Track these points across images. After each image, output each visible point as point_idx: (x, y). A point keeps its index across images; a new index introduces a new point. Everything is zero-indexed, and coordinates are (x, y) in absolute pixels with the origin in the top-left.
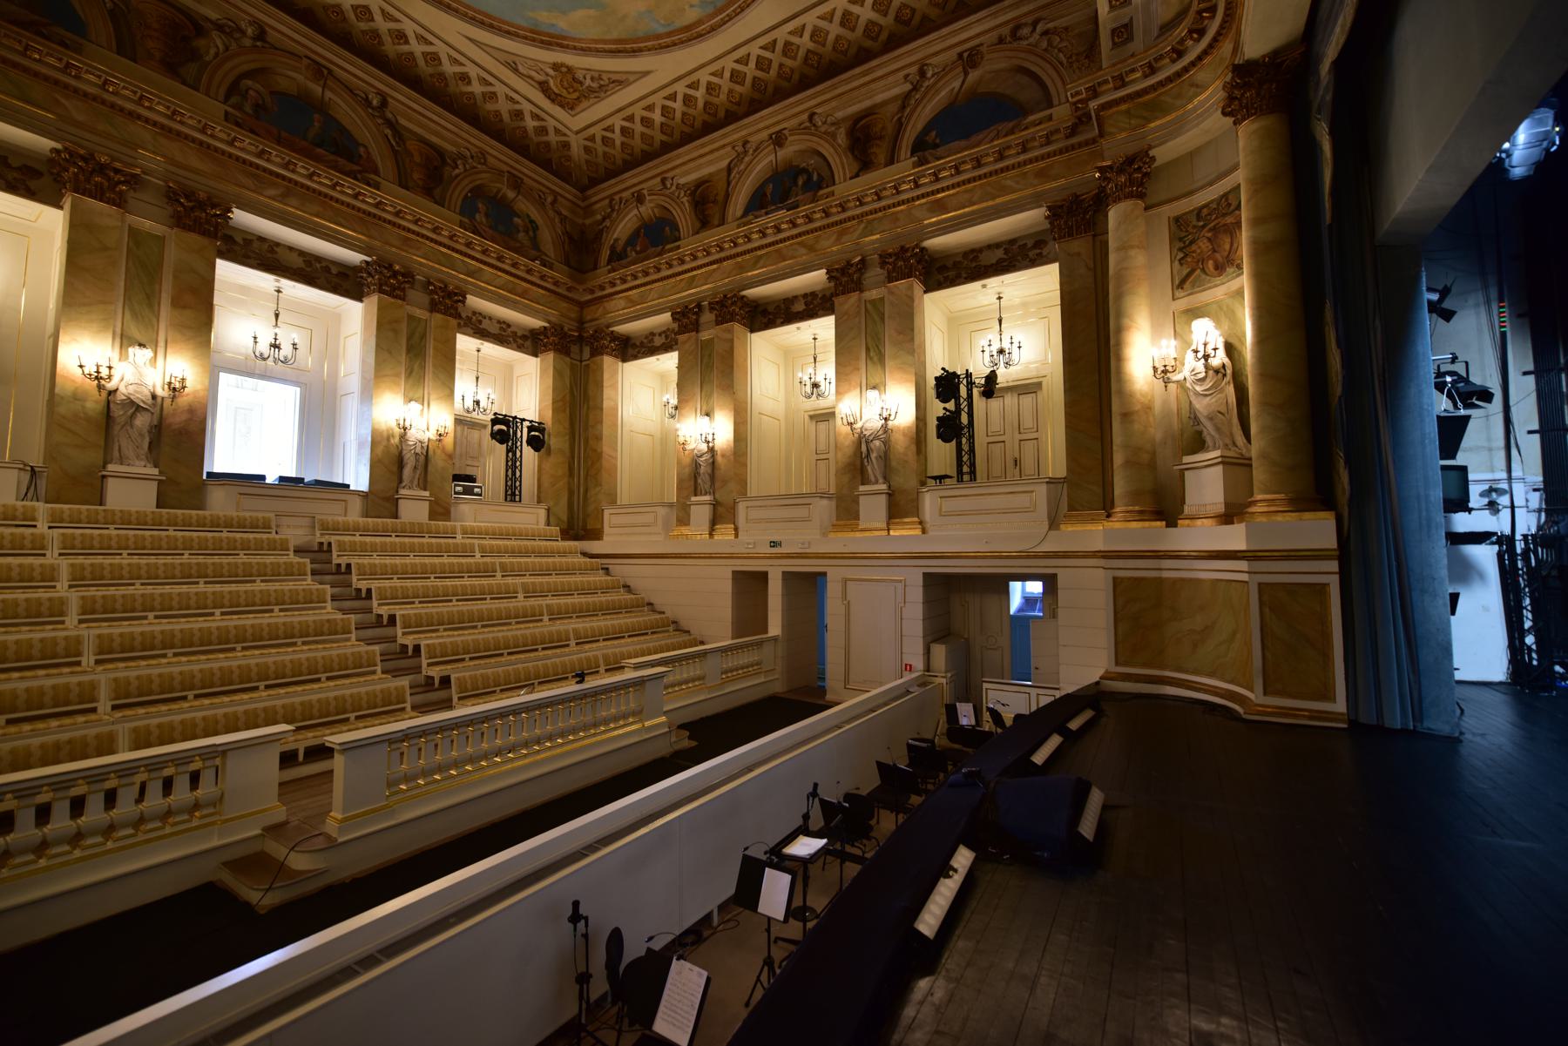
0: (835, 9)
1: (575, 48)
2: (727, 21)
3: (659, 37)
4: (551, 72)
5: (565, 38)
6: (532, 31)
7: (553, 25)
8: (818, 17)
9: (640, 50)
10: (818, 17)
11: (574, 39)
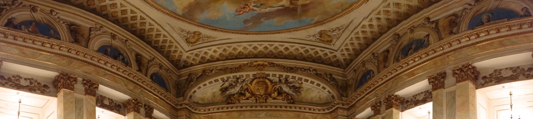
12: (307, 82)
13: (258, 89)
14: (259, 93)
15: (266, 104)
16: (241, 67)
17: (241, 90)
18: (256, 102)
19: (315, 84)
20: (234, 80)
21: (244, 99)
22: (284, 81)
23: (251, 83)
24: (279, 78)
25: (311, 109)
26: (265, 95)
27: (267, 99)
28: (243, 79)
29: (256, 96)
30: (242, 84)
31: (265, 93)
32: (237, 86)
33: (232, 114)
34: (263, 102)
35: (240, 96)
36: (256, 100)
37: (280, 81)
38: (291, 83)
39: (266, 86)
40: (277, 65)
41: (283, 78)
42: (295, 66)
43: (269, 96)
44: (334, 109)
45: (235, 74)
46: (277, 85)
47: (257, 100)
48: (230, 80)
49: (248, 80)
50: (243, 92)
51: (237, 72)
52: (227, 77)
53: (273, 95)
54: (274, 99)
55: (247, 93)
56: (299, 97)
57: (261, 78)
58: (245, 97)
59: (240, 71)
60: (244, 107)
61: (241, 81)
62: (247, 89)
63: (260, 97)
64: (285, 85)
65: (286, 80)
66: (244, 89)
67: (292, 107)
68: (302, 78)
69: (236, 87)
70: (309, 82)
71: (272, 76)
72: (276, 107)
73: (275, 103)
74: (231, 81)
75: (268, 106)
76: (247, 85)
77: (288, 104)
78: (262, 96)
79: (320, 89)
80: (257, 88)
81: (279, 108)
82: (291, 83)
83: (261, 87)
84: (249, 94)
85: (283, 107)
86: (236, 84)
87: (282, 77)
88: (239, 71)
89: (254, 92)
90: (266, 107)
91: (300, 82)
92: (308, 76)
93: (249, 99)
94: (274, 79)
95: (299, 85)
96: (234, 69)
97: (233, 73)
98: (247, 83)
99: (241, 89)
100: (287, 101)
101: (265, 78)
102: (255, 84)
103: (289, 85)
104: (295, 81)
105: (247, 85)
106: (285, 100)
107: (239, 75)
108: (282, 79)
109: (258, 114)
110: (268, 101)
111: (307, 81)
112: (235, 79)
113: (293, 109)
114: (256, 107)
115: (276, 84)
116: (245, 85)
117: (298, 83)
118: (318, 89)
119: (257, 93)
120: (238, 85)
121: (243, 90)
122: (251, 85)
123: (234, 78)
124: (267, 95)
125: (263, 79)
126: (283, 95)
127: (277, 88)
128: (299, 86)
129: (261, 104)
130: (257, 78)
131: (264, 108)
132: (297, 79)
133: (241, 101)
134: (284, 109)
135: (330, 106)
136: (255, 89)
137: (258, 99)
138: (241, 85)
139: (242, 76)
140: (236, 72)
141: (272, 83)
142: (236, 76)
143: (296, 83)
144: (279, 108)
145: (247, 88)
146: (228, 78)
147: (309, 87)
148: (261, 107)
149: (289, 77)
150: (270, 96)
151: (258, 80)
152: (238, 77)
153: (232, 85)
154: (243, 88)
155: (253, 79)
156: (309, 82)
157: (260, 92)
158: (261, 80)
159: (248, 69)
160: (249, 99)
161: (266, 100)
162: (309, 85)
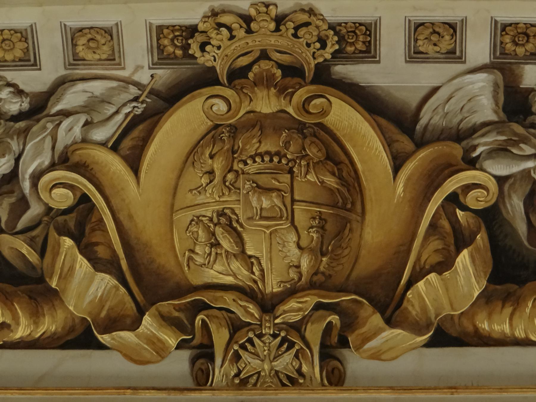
14: (236, 265)
27: (344, 343)
29: (204, 307)
30: (15, 145)
39: (331, 181)
43: (367, 309)
47: (211, 358)
50: (25, 249)
83: (267, 190)
93: (104, 339)
94: (435, 90)
116: (52, 167)
121: (21, 224)
124: (342, 290)
141: (420, 144)
145: (84, 199)
151: (220, 106)
155: (152, 92)
160: (104, 339)
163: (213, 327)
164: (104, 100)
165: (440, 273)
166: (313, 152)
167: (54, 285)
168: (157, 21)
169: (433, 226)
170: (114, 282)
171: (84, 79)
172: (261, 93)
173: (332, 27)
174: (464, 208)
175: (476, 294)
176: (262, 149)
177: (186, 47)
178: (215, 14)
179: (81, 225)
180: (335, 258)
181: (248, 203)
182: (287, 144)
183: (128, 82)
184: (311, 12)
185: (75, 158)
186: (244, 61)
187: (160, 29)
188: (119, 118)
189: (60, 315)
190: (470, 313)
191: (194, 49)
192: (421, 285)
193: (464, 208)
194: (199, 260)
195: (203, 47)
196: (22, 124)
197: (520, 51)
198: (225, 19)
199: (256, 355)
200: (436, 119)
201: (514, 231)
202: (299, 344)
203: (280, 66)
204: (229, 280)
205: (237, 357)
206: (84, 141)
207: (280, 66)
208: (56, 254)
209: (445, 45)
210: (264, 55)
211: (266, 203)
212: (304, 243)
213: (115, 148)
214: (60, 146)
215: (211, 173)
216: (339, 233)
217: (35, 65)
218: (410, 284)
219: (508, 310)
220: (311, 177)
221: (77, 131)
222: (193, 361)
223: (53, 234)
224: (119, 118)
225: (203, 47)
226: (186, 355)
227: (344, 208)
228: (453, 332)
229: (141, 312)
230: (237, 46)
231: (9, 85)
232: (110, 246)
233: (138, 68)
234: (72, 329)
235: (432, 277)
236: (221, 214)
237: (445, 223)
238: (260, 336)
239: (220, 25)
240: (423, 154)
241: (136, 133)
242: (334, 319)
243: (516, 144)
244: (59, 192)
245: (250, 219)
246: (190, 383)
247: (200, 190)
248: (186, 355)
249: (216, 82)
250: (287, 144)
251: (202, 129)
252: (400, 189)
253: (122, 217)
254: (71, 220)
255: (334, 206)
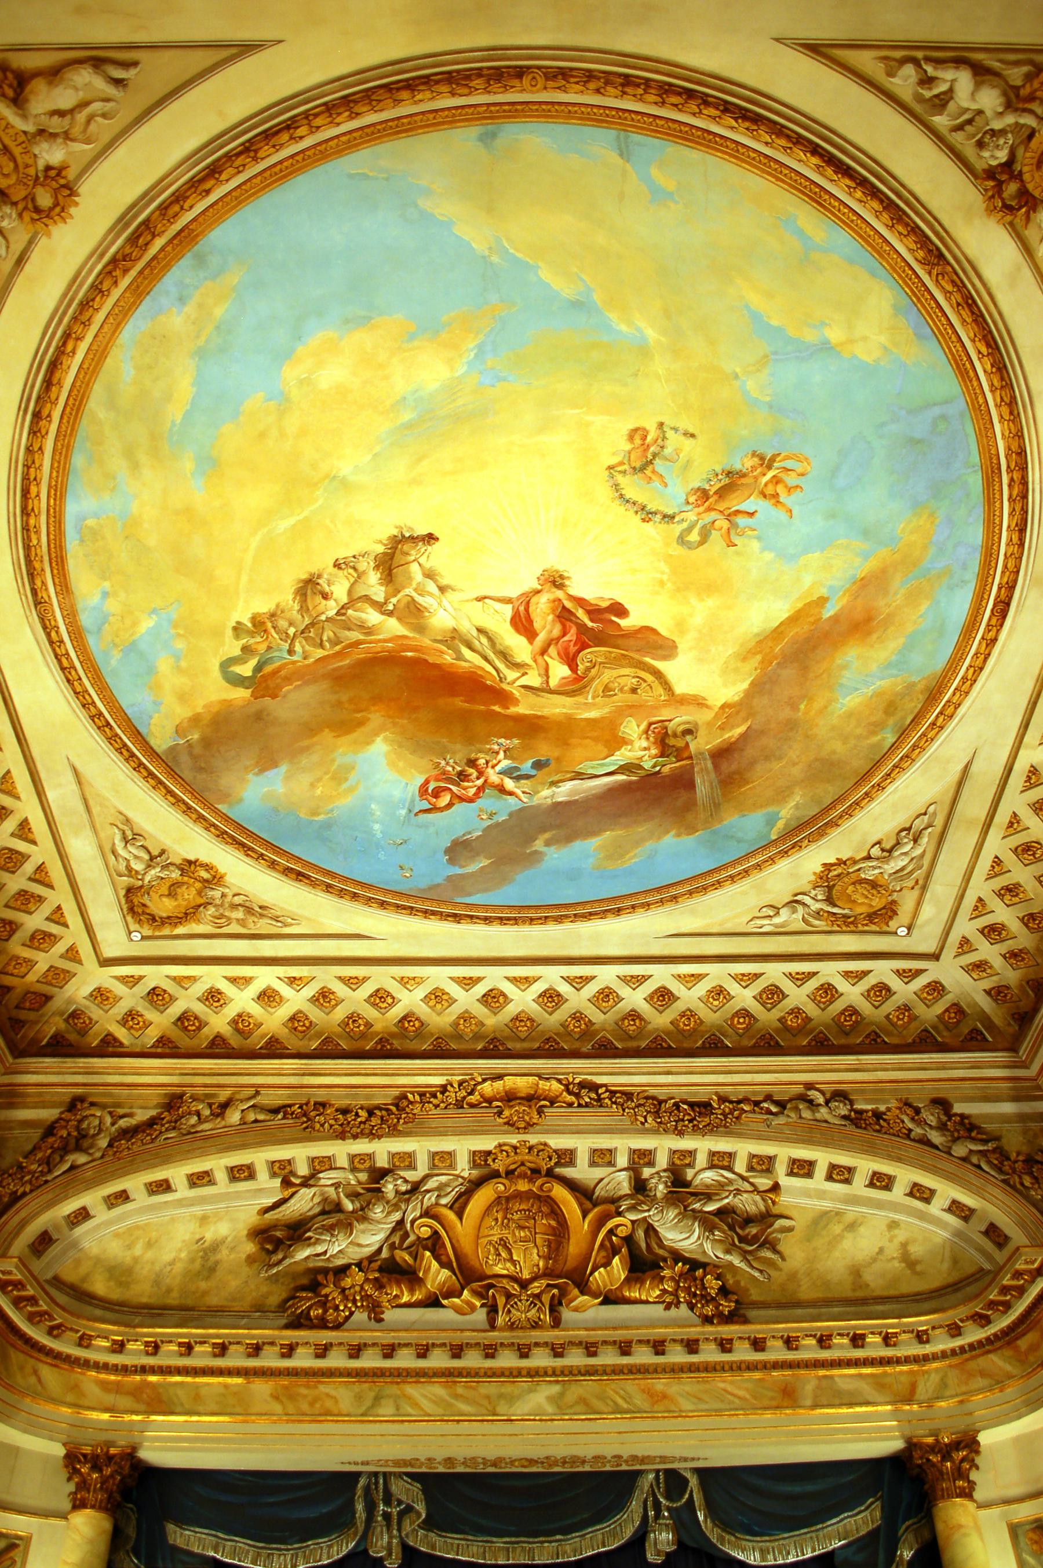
0: (18, 798)
1: (98, 290)
2: (48, 635)
3: (58, 492)
4: (52, 154)
5: (139, 292)
6: (187, 238)
7: (182, 300)
8: (8, 772)
9: (35, 432)
10: (8, 772)
11: (122, 314)
12: (809, 1175)
13: (504, 1243)
14: (509, 1265)
15: (556, 1332)
16: (405, 1103)
17: (392, 1247)
18: (492, 1326)
19: (860, 1180)
20: (353, 1182)
21: (405, 1299)
22: (661, 1187)
23: (459, 1206)
24: (634, 1168)
25: (863, 1337)
26: (544, 1282)
27: (560, 1304)
28: (412, 1176)
29: (491, 1286)
31: (546, 1268)
32: (364, 1219)
33: (322, 1388)
34: (535, 1325)
35: (385, 1280)
36: (493, 1310)
37: (640, 1187)
38: (709, 1197)
39: (553, 1223)
40: (613, 1093)
41: (653, 1170)
42: (720, 1089)
43: (571, 1285)
44: (1020, 1307)
45: (362, 1146)
46: (619, 1214)
47: (497, 1312)
48: (327, 1178)
49: (440, 1188)
50: (407, 1257)
51: (380, 1137)
52: (312, 1160)
53: (599, 1277)
54: (609, 1299)
55: (435, 1265)
56: (773, 1273)
57: (523, 1176)
58: (412, 1291)
59: (400, 1128)
60: (405, 1351)
61: (397, 1192)
62: (434, 1244)
63: (514, 1288)
64: (672, 1214)
65: (677, 1179)
66: (412, 1238)
67: (730, 1341)
68: (771, 1159)
69: (358, 1227)
70: (821, 1171)
71: (593, 1164)
72: (625, 1348)
73: (615, 1328)
74: (336, 1185)
75: (571, 1343)
76: (436, 1217)
77: (709, 1329)
78: (524, 1285)
79: (894, 1207)
80: (496, 1234)
81: (643, 1356)
82: (708, 1196)
83: (522, 1228)
84: (445, 1273)
85: (669, 1347)
86: (362, 1209)
87: (651, 1164)
88: (394, 1132)
89: (474, 1263)
90: (557, 1351)
91: (764, 1182)
92: (808, 1141)
93: (445, 1302)
94: (602, 1180)
95: (758, 1198)
96: (363, 1114)
97: (355, 1137)
98: (437, 1204)
99: (396, 1239)
100: (691, 1307)
101: (550, 1173)
102: (488, 1211)
103: (697, 1206)
104: (730, 1182)
105: (436, 1217)
106: (678, 1304)
107: (393, 1156)
108: (652, 1176)
109: (501, 1396)
110: (566, 1314)
111: (802, 1168)
112: (363, 1176)
113: (743, 1353)
114: (490, 1351)
115: (612, 1208)
116: (421, 1217)
117: (756, 1190)
118: (879, 1205)
119: (499, 1269)
120: (378, 1211)
121: (405, 1246)
122: (460, 1215)
123: (354, 1170)
124: (559, 1277)
125: (531, 1180)
126: (666, 1273)
127: (622, 1232)
128: (763, 1208)
129: (520, 1333)
130: (495, 1175)
131: (541, 1359)
132: (740, 1166)
133: (390, 1315)
134: (677, 1356)
135: (993, 1295)
136: (484, 1241)
137: (501, 1301)
138: (397, 1216)
139: (408, 1160)
140: (373, 1135)
141: (595, 1205)
142: (371, 1156)
143: (738, 1192)
144: (643, 1356)
145: (436, 1233)
146: (321, 1164)
147: (826, 1205)
148: (524, 1352)
149: (695, 1159)
150: (584, 1287)
151: (501, 1187)
152: (382, 1162)
153: (338, 1208)
154: (406, 1235)
155: (470, 1181)
156: (821, 1171)
157: (514, 1263)
158: (523, 1186)
159: (449, 1123)
160: (445, 1302)
161: (555, 1307)
162: (821, 1195)
163: (497, 1297)
164: (447, 1185)
165: (605, 1268)
166: (544, 1209)
167: (421, 1275)
168: (473, 1148)
169: (602, 1245)
170: (450, 1273)
171: (437, 1175)
172: (520, 1181)
173: (555, 1151)
174: (616, 1236)
175: (623, 1278)
176: (521, 1207)
177: (486, 1161)
178: (500, 1145)
179: (434, 1245)
180: (555, 1261)
181: (514, 1234)
182: (532, 1206)
183: (458, 1176)
184: (545, 1144)
185: (432, 1213)
186: (513, 1167)
187: (474, 1152)
188: (454, 1193)
189: (424, 1290)
190: (620, 1288)
191: (490, 1161)
192: (596, 1274)
193: (616, 1236)
194: (491, 1262)
195: (494, 1160)
196: (407, 1196)
197: (642, 1162)
198: (504, 1148)
199: (518, 1310)
200: (603, 1193)
201: (640, 1247)
202: (539, 1304)
203: (530, 1169)
204: (505, 1272)
205: (509, 1311)
206: (437, 1204)
207: (530, 1169)
208: (422, 1260)
209: (607, 1159)
210: (523, 1164)
211: (522, 1234)
212: (541, 1254)
213: (451, 1208)
214: (425, 1207)
215: (496, 1219)
216: (557, 1249)
217: (415, 1169)
218: (592, 1273)
219: (638, 1286)
220: (544, 1221)
221: (433, 1199)
222: (488, 1313)
223: (421, 1250)
224: (454, 1193)
225: (494, 1160)
226: (484, 1310)
227: (559, 1236)
228: (612, 1297)
229: (463, 1289)
230: (511, 1159)
231: (401, 1178)
232: (448, 1256)
233: (463, 1170)
234: (430, 1297)
235: (602, 1270)
236: (501, 1239)
237: (607, 1244)
238: (520, 1301)
239: (502, 1151)
240: (596, 1210)
241: (461, 1200)
242: (555, 1291)
243: (640, 1205)
244: (423, 1229)
245: (515, 1242)
246: (488, 1327)
247: (492, 1228)
248: (484, 1310)
249: (499, 1176)
250: (532, 1206)
251: (493, 1198)
252: (586, 1226)
253: (454, 1241)
254: (429, 1243)
255: (554, 1235)
